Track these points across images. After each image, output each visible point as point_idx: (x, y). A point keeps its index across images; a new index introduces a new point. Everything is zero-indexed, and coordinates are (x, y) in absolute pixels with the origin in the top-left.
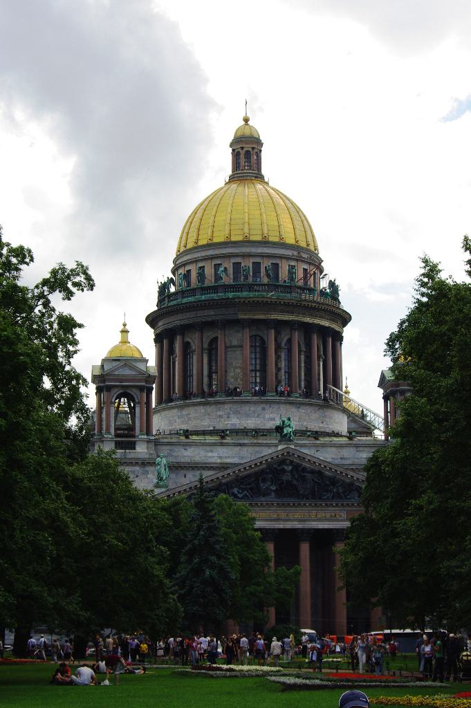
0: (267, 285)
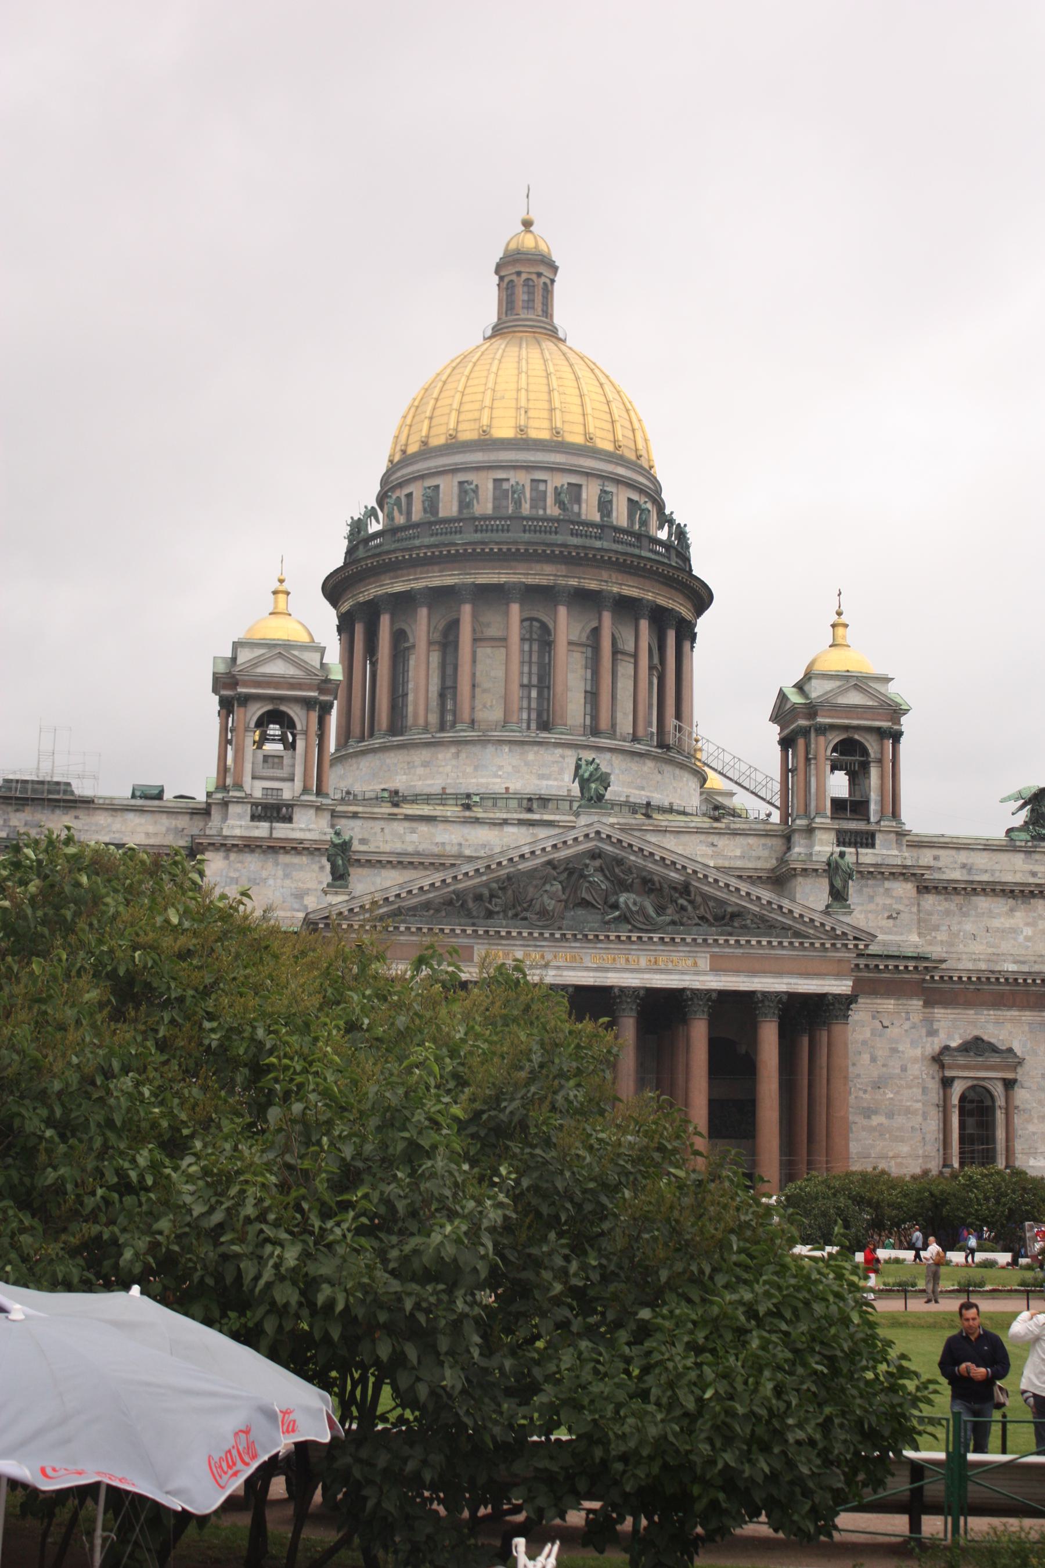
0: (558, 521)
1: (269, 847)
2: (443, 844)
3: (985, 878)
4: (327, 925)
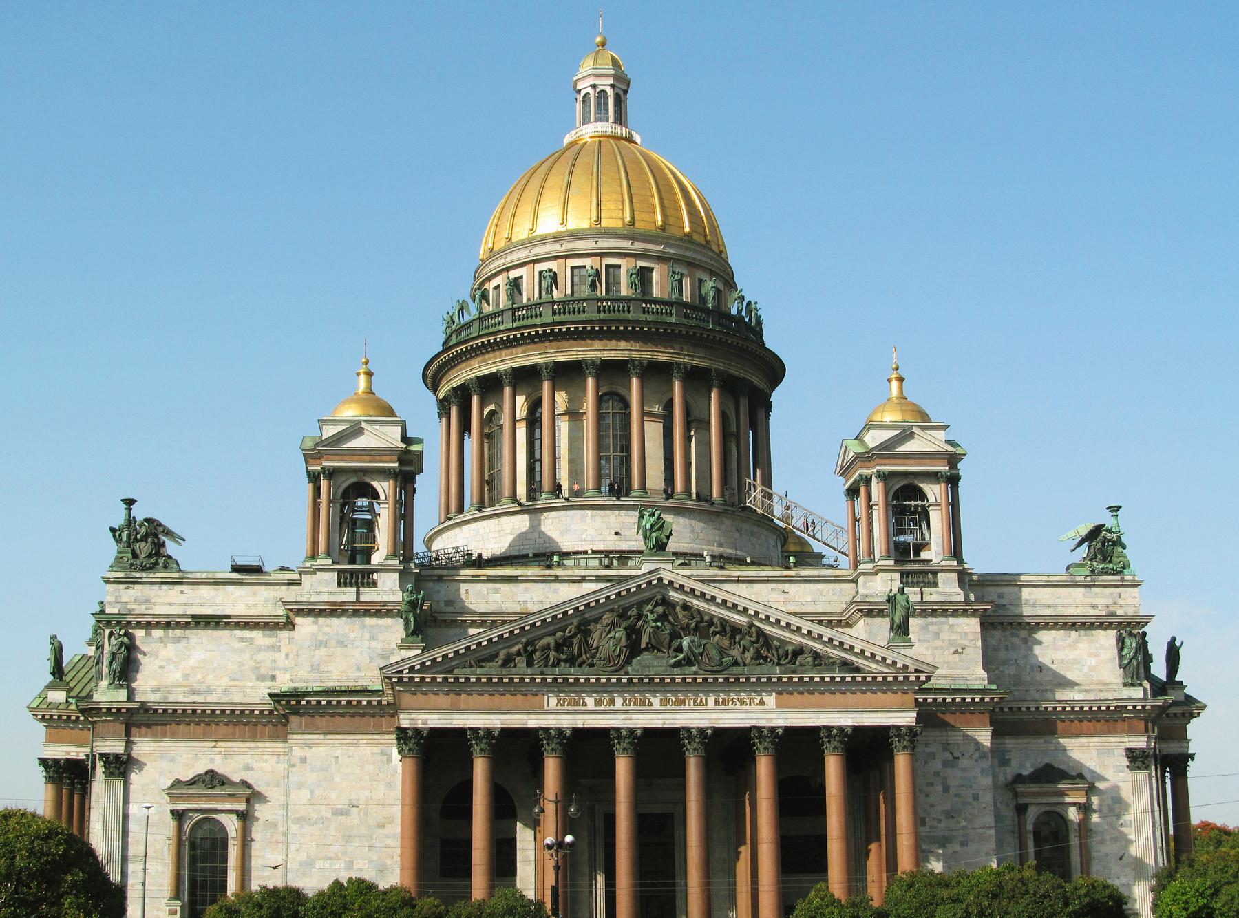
2: (525, 602)
3: (1048, 612)
4: (400, 679)
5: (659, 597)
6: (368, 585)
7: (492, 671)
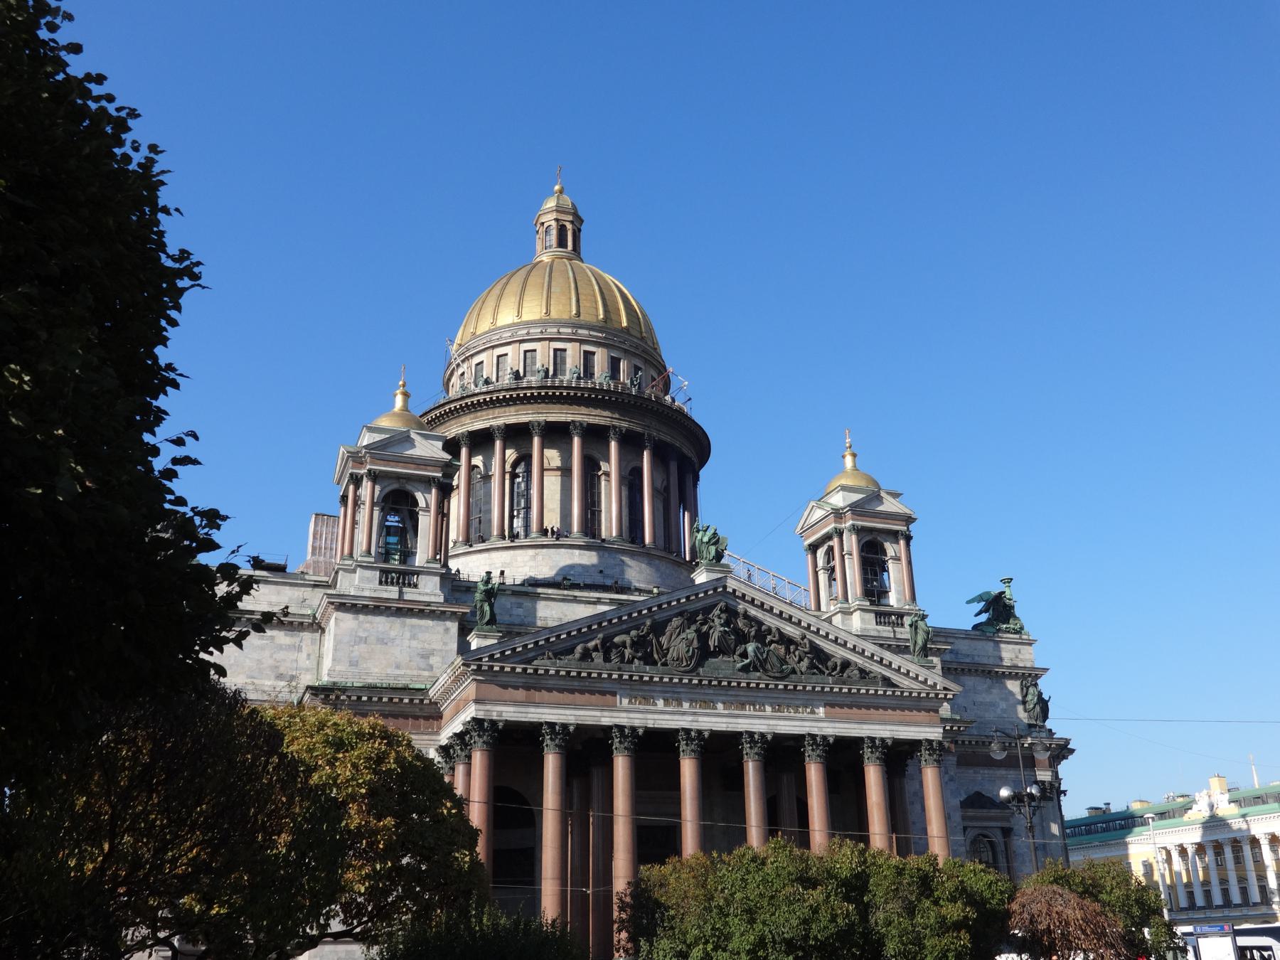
1: (399, 609)
3: (968, 660)
4: (480, 667)
5: (722, 604)
6: (409, 585)
7: (569, 665)
